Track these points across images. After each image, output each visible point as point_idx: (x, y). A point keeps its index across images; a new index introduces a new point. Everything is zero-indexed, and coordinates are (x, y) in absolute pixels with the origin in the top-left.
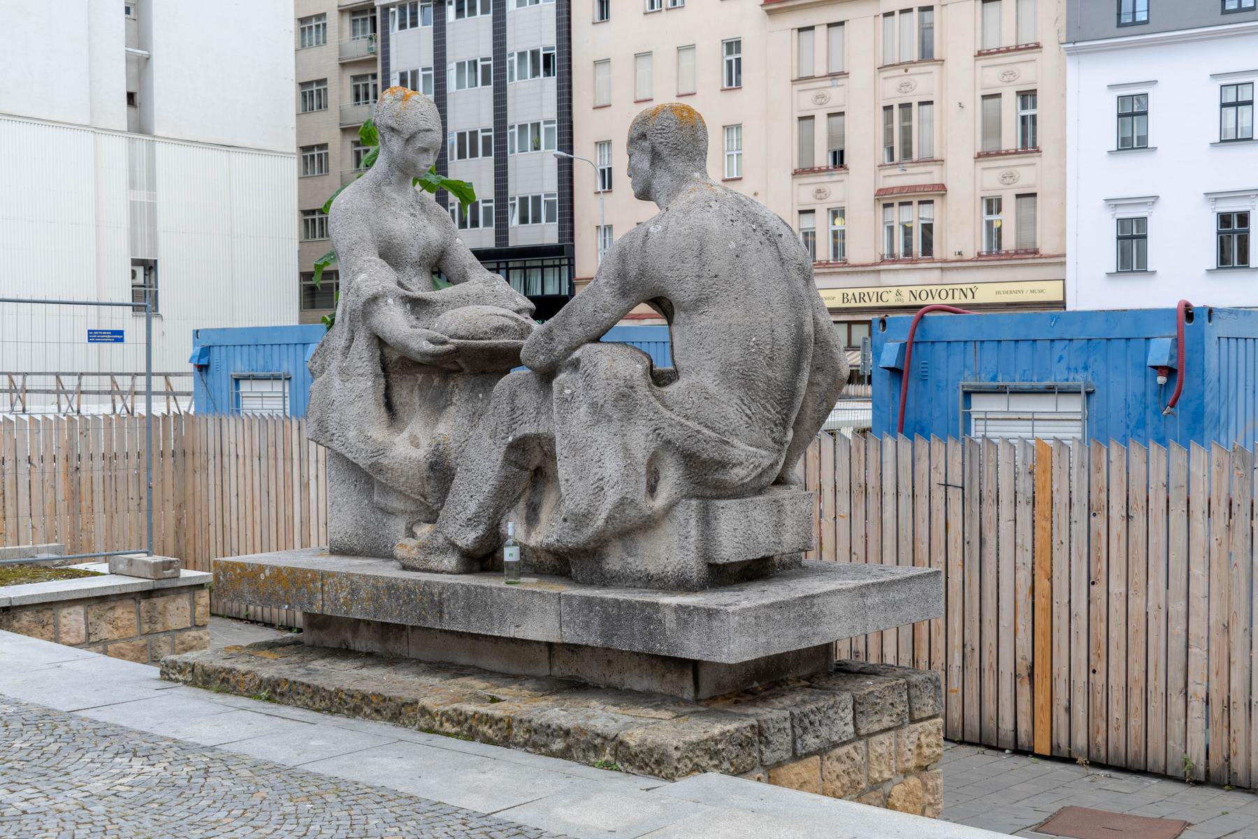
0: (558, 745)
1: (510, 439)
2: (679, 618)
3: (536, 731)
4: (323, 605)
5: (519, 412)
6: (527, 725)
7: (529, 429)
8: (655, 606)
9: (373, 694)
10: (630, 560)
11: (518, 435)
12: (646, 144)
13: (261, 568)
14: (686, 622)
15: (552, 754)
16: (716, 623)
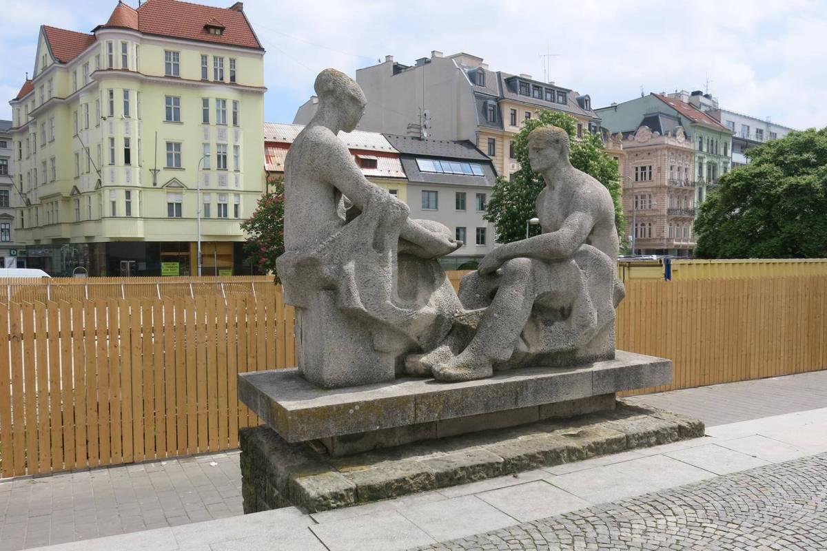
0: (653, 439)
1: (536, 295)
2: (652, 369)
3: (642, 438)
4: (415, 418)
5: (538, 281)
6: (637, 436)
7: (546, 289)
8: (639, 367)
9: (538, 453)
10: (589, 350)
11: (541, 293)
12: (560, 146)
13: (353, 405)
14: (654, 370)
15: (650, 445)
16: (667, 368)
